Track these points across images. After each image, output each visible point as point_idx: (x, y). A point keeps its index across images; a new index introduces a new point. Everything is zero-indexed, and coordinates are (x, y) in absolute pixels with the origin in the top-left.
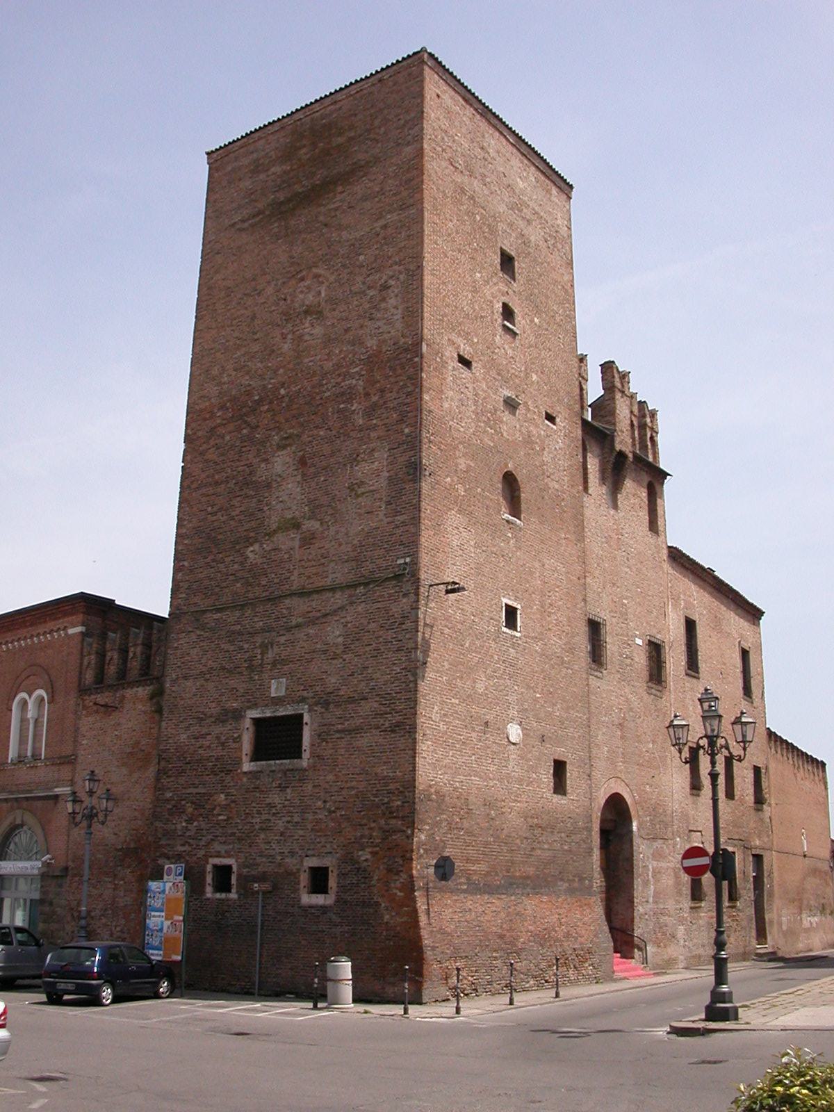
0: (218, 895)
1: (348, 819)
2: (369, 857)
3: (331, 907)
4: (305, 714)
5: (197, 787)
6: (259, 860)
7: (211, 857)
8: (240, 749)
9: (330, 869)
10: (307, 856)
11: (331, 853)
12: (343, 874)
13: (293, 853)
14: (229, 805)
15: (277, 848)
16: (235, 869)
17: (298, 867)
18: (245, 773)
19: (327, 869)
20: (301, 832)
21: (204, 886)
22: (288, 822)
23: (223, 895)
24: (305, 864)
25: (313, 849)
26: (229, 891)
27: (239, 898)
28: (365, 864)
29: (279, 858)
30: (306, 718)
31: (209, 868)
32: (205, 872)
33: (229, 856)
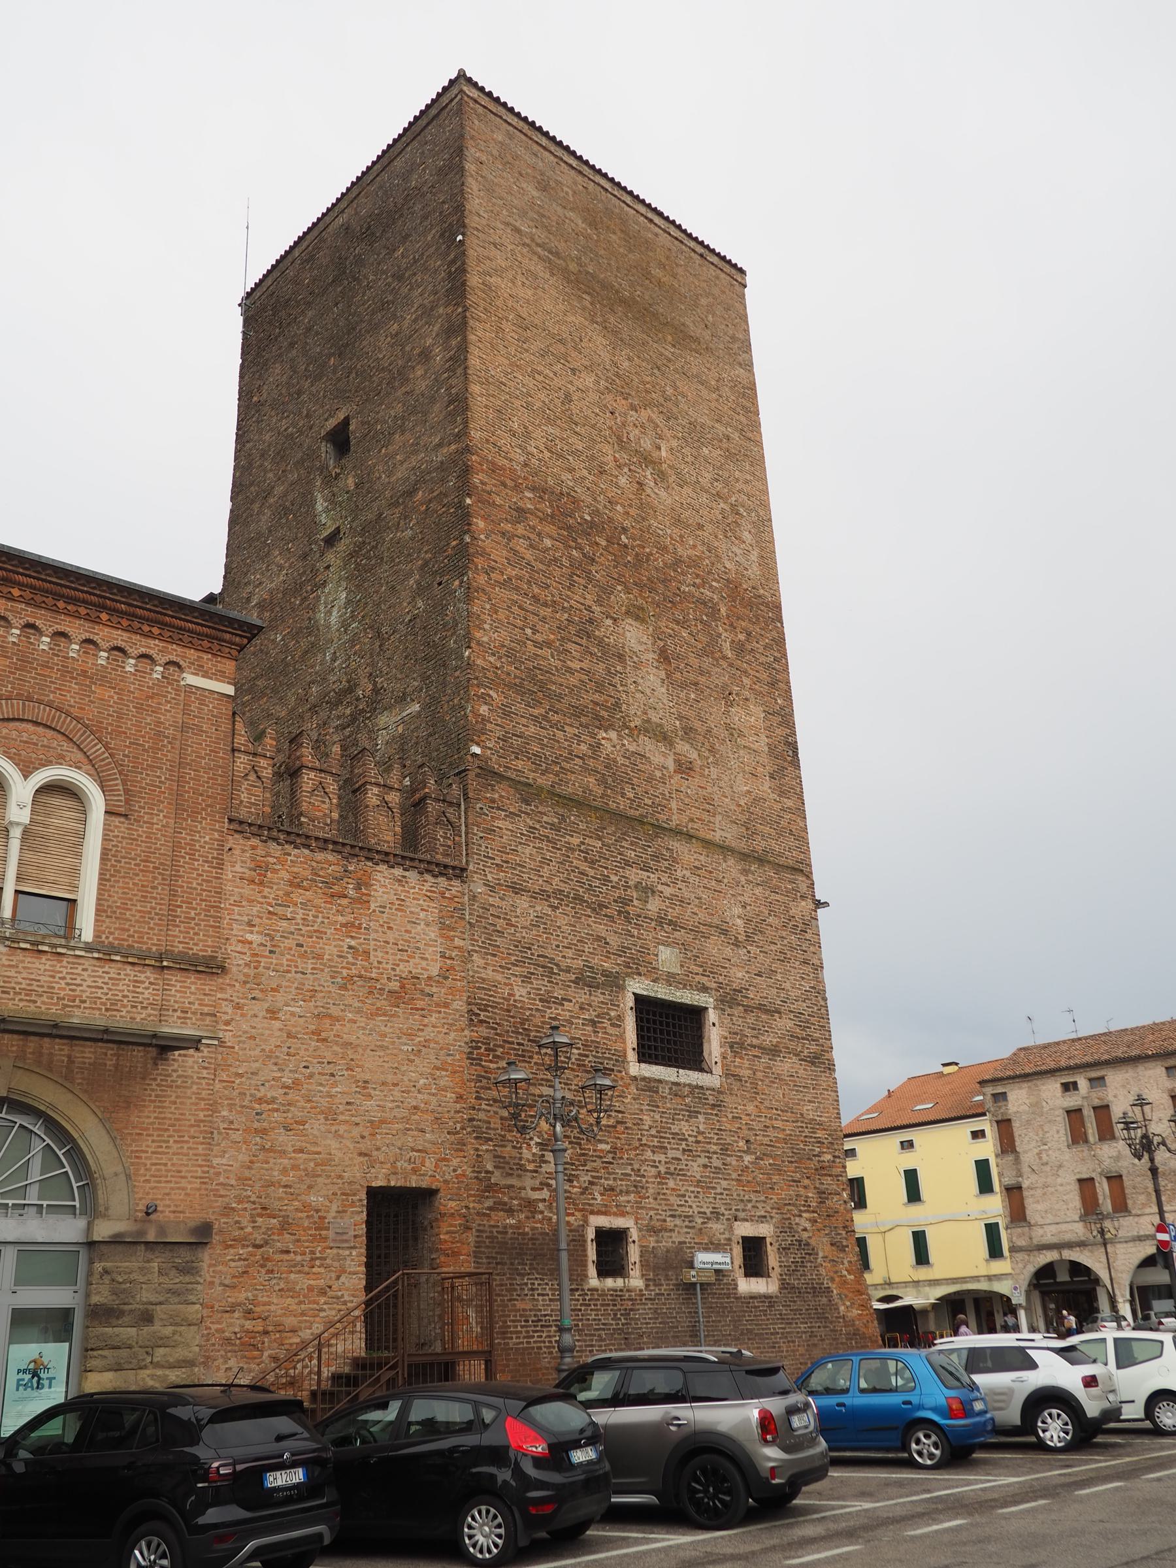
1: (779, 1171)
2: (808, 1225)
6: (670, 1222)
7: (592, 1213)
8: (622, 1037)
9: (768, 1240)
11: (765, 1217)
12: (784, 1249)
13: (718, 1213)
14: (615, 1127)
15: (694, 1206)
16: (634, 1234)
17: (727, 1236)
18: (635, 1078)
20: (724, 1184)
22: (705, 1166)
23: (620, 1282)
24: (736, 1232)
27: (647, 1286)
29: (700, 1221)
30: (712, 1016)
31: (591, 1234)
32: (585, 1241)
33: (623, 1214)
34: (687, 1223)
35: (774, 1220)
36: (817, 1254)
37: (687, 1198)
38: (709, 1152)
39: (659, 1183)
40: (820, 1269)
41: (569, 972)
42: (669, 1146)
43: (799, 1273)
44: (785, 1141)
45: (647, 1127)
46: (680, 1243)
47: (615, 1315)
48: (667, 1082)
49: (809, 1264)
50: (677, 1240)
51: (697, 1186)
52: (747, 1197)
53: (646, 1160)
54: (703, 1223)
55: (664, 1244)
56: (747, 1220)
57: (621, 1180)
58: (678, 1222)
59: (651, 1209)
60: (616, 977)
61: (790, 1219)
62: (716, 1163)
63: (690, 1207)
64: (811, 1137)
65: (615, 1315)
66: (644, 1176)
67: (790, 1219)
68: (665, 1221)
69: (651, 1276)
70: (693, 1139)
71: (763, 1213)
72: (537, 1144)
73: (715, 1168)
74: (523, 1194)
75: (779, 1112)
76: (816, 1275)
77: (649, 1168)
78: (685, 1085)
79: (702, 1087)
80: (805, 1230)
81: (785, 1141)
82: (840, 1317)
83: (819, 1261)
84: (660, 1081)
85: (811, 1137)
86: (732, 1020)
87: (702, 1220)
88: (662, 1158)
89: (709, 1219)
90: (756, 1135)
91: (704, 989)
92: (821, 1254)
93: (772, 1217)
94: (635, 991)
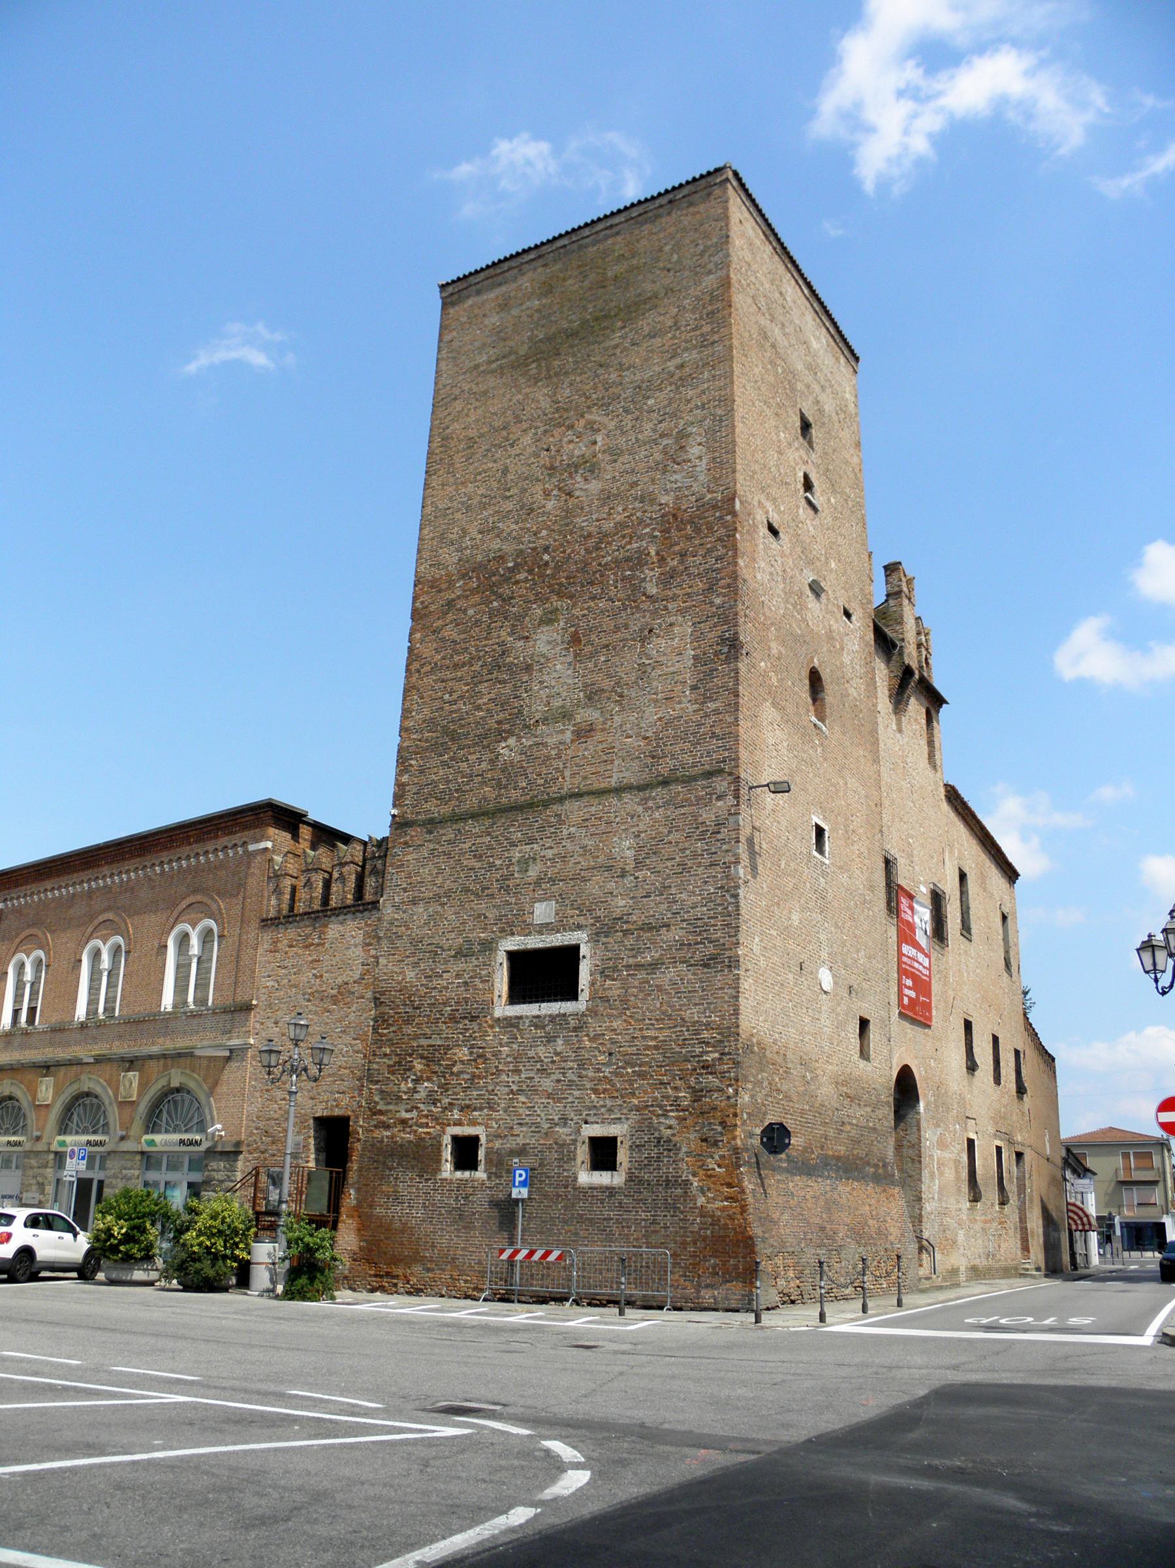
0: (459, 1174)
3: (619, 1188)
4: (582, 946)
5: (430, 1038)
7: (449, 1125)
9: (619, 1140)
10: (586, 1123)
11: (620, 1119)
12: (637, 1146)
15: (542, 1115)
16: (483, 1139)
18: (499, 1019)
19: (614, 1139)
20: (577, 1093)
21: (438, 1161)
22: (559, 1081)
23: (467, 1174)
24: (582, 1134)
25: (595, 1115)
26: (476, 1170)
27: (489, 1178)
28: (669, 1132)
29: (546, 1126)
30: (584, 950)
31: (447, 1140)
34: (533, 1129)
35: (629, 1122)
36: (679, 1149)
37: (536, 1109)
38: (564, 1068)
39: (510, 1099)
40: (680, 1163)
41: (449, 950)
42: (523, 1069)
43: (652, 1168)
44: (656, 1048)
45: (504, 1056)
46: (524, 1144)
47: (457, 1198)
48: (527, 1017)
49: (665, 1160)
50: (521, 1142)
51: (548, 1098)
52: (601, 1103)
53: (501, 1082)
54: (549, 1128)
55: (508, 1145)
56: (597, 1123)
57: (476, 1099)
58: (524, 1129)
59: (500, 1119)
60: (490, 943)
61: (651, 1119)
62: (570, 1075)
63: (539, 1115)
64: (692, 1039)
65: (457, 1198)
66: (496, 1095)
67: (651, 1119)
68: (512, 1128)
69: (494, 1170)
70: (550, 1060)
71: (618, 1116)
72: (413, 1080)
73: (569, 1081)
74: (398, 1115)
75: (653, 1022)
76: (674, 1169)
77: (503, 1088)
78: (545, 1016)
79: (564, 1015)
80: (670, 1127)
81: (656, 1048)
82: (696, 1208)
83: (680, 1156)
84: (521, 1018)
85: (692, 1039)
86: (606, 947)
87: (549, 1125)
88: (516, 1078)
89: (556, 1125)
90: (621, 1047)
91: (579, 927)
92: (684, 1149)
93: (627, 1119)
94: (507, 949)
